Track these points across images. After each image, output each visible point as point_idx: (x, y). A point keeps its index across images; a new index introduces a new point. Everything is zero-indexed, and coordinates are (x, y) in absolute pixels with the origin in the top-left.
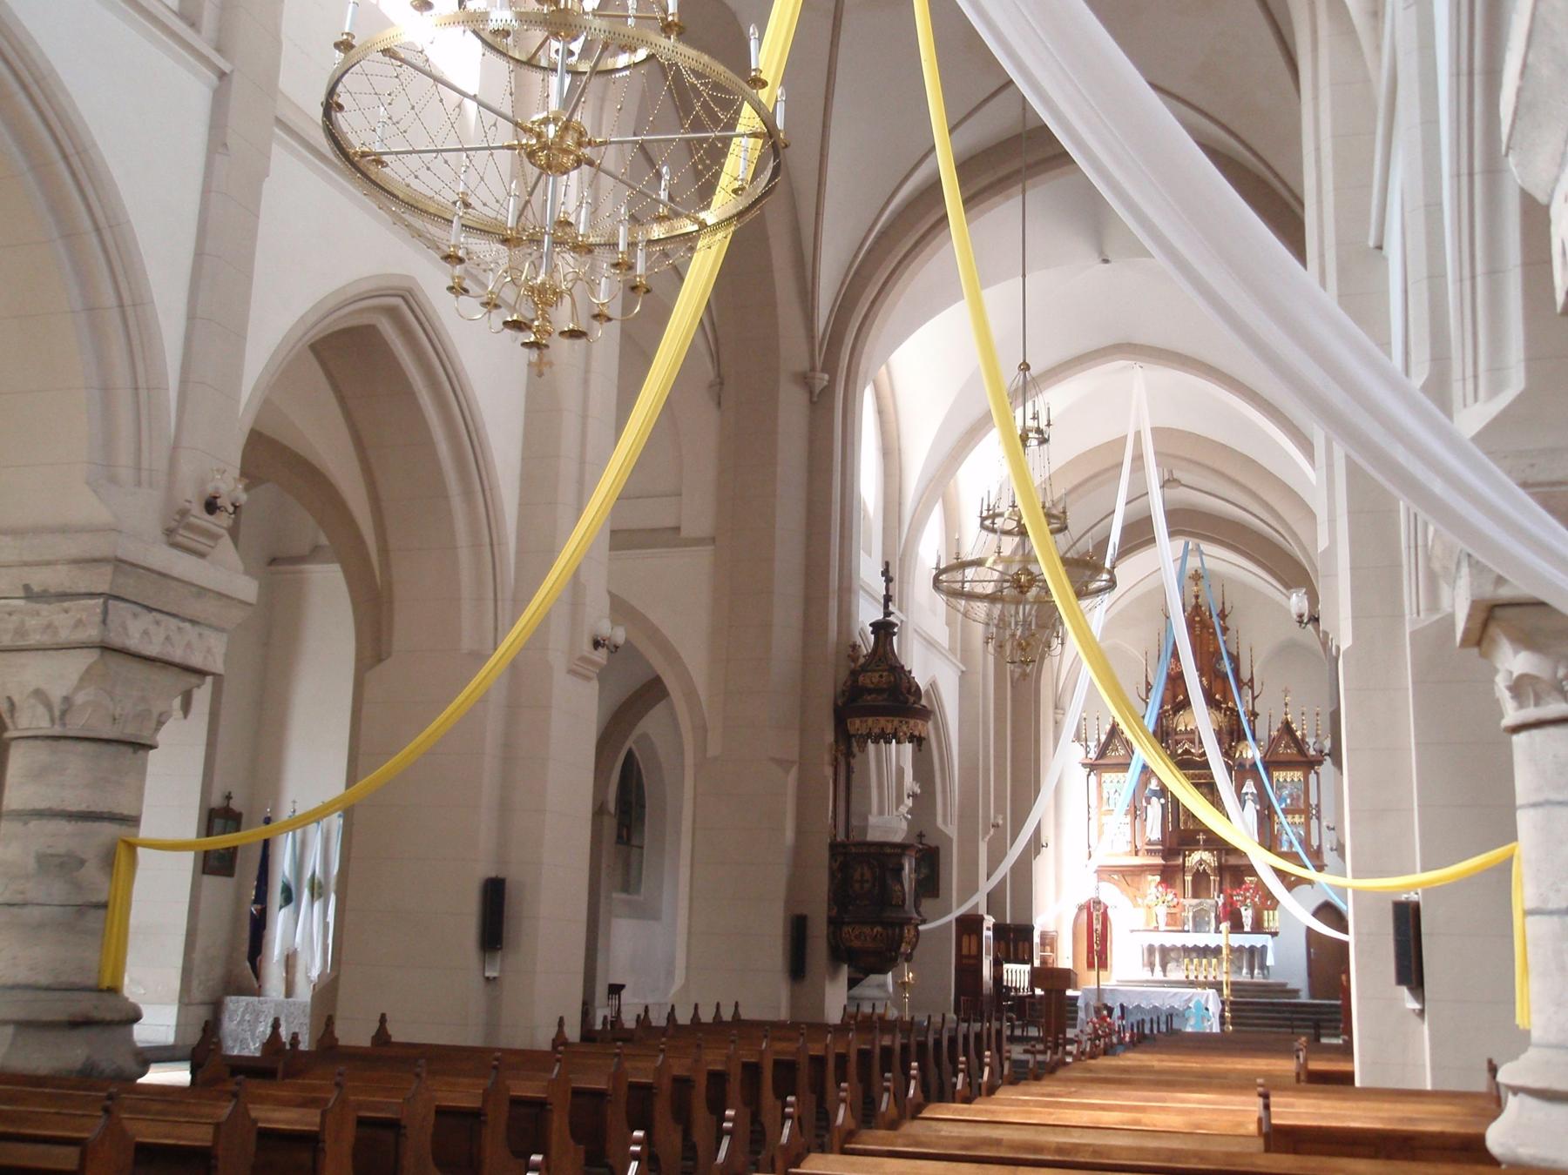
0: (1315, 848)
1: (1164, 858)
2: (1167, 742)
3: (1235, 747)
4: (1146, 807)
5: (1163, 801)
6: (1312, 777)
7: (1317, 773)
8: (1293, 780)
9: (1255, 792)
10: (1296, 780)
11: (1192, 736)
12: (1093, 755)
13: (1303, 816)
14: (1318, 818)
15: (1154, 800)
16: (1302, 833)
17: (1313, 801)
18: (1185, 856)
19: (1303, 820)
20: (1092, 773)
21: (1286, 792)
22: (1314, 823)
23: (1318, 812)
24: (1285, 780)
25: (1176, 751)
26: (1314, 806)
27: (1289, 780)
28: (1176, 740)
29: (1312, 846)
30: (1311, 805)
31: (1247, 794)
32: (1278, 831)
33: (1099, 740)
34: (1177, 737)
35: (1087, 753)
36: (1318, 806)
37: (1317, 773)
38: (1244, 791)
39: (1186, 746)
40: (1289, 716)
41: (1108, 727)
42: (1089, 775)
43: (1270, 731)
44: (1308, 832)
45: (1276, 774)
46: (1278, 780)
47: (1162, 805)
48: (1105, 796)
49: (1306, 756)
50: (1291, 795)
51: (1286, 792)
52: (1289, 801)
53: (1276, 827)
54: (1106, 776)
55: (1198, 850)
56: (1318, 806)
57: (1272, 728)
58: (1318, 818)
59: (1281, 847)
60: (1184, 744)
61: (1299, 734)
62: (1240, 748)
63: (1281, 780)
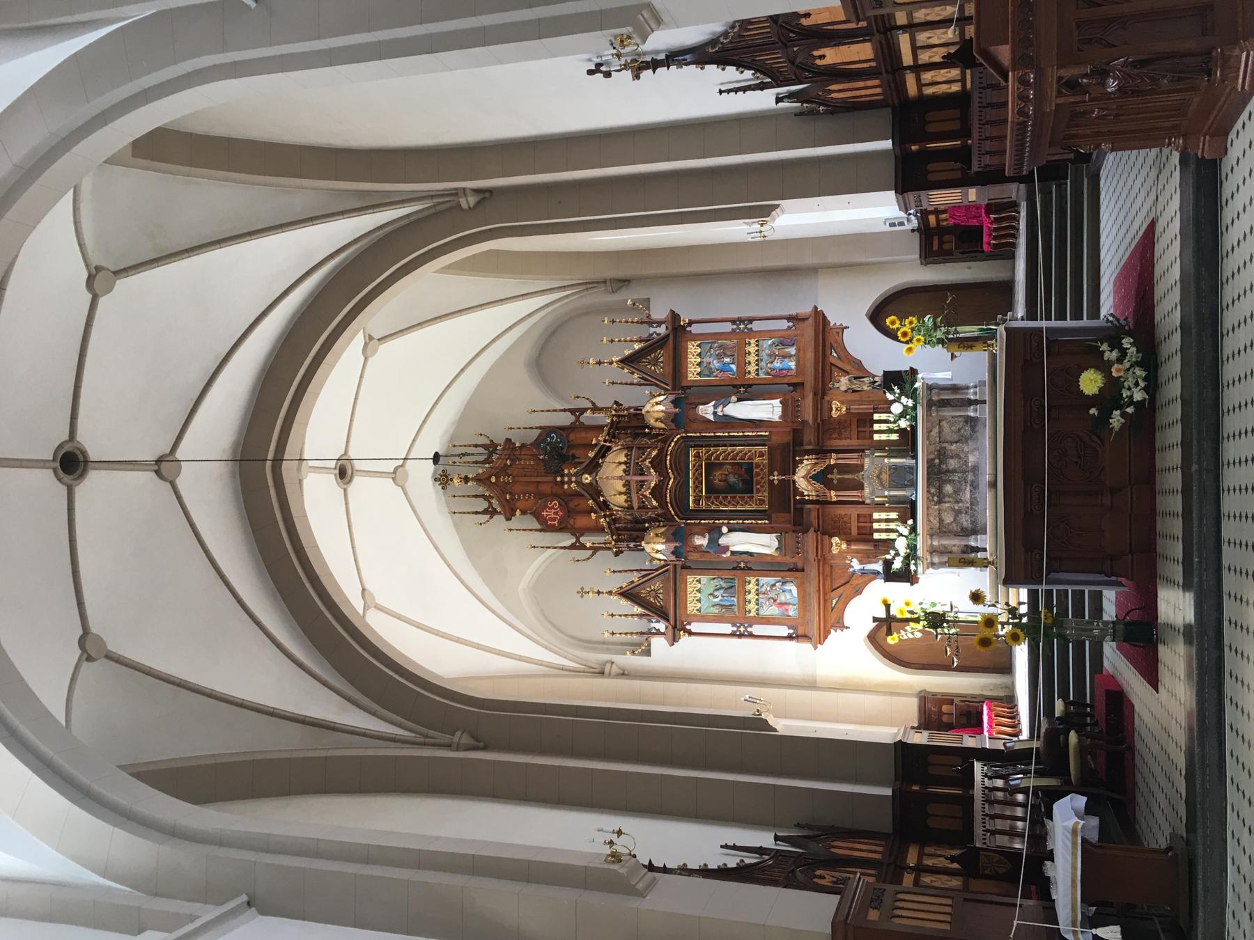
0: (791, 324)
1: (806, 531)
2: (645, 521)
3: (651, 428)
4: (733, 553)
5: (725, 529)
6: (695, 329)
7: (691, 323)
8: (699, 355)
9: (713, 403)
10: (699, 350)
11: (633, 486)
12: (661, 626)
13: (748, 340)
14: (751, 320)
15: (723, 541)
16: (770, 342)
17: (728, 327)
18: (803, 502)
19: (753, 341)
20: (688, 627)
21: (716, 364)
22: (756, 326)
23: (741, 320)
24: (699, 364)
25: (655, 508)
26: (735, 327)
27: (699, 360)
28: (639, 508)
29: (789, 328)
30: (734, 330)
31: (715, 413)
32: (768, 374)
33: (641, 615)
34: (636, 506)
35: (658, 633)
36: (733, 322)
37: (691, 323)
38: (711, 418)
39: (647, 493)
40: (614, 359)
41: (624, 602)
42: (690, 633)
43: (632, 384)
44: (770, 334)
45: (691, 377)
46: (699, 374)
47: (730, 531)
48: (716, 610)
49: (667, 336)
50: (719, 357)
51: (716, 364)
52: (727, 360)
53: (762, 376)
54: (691, 608)
55: (794, 482)
56: (733, 322)
57: (629, 381)
58: (751, 320)
59: (790, 369)
60: (645, 496)
61: (637, 346)
62: (652, 422)
63: (699, 370)
